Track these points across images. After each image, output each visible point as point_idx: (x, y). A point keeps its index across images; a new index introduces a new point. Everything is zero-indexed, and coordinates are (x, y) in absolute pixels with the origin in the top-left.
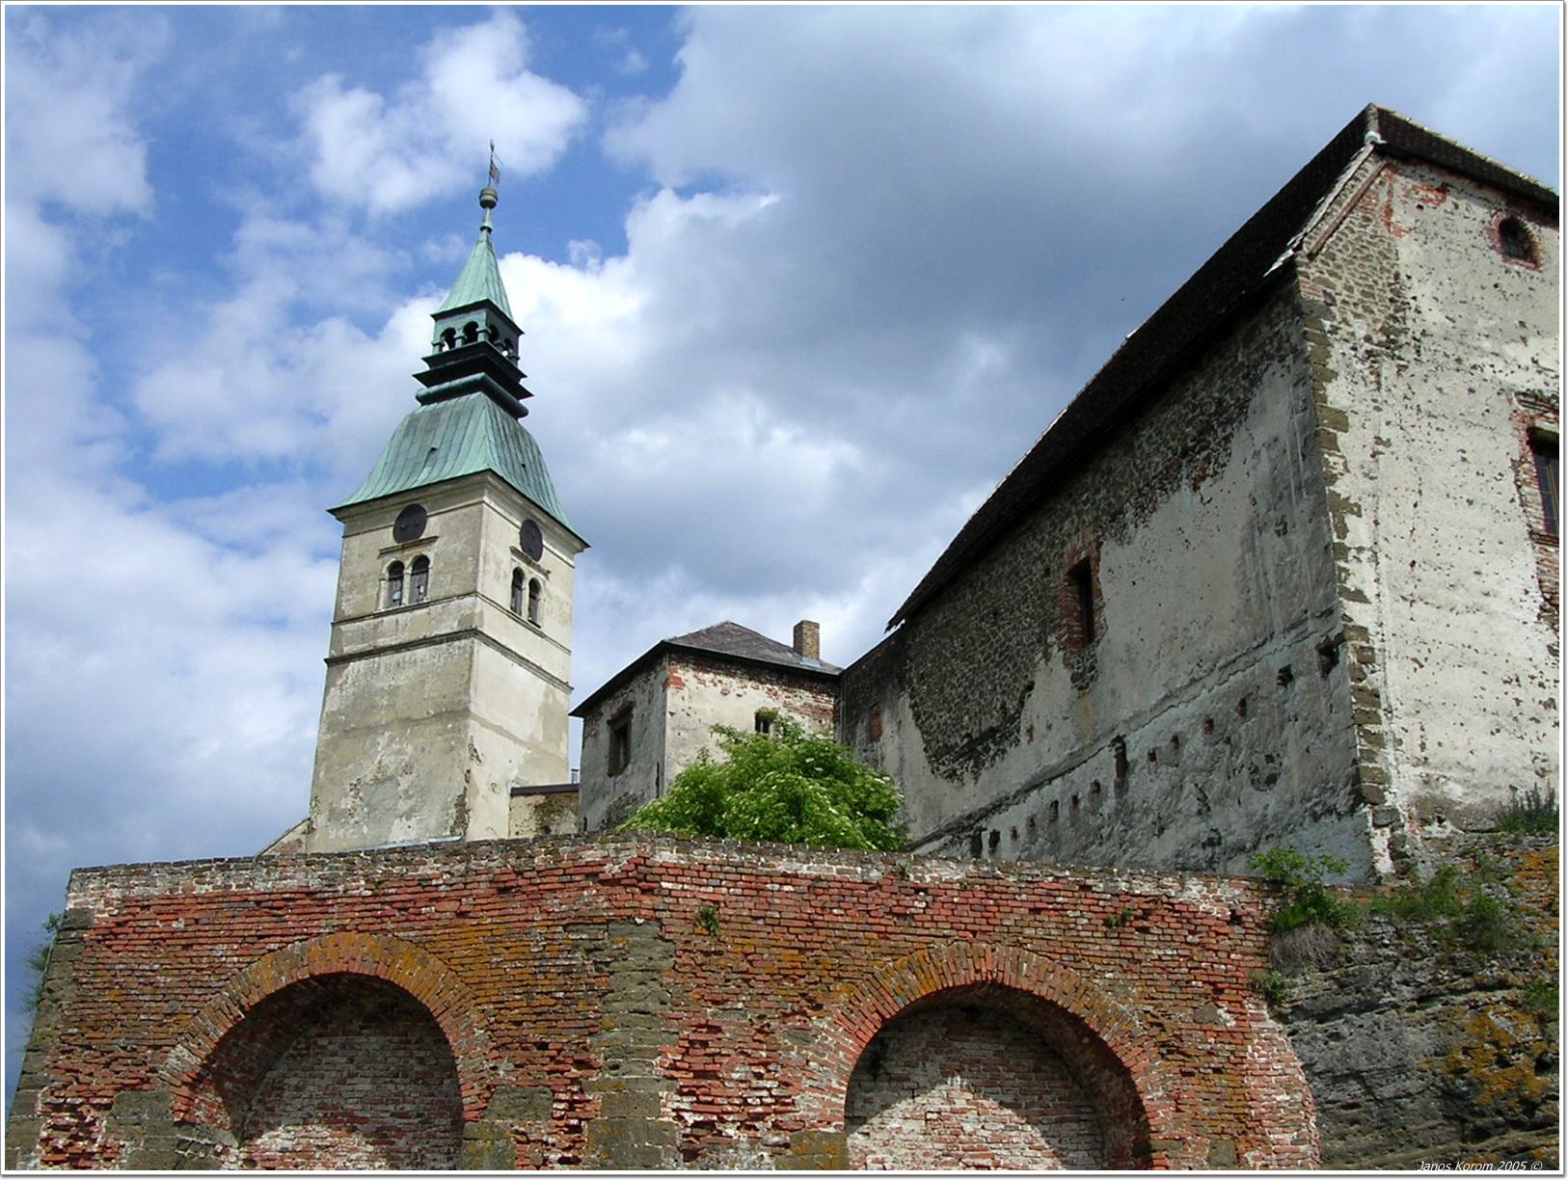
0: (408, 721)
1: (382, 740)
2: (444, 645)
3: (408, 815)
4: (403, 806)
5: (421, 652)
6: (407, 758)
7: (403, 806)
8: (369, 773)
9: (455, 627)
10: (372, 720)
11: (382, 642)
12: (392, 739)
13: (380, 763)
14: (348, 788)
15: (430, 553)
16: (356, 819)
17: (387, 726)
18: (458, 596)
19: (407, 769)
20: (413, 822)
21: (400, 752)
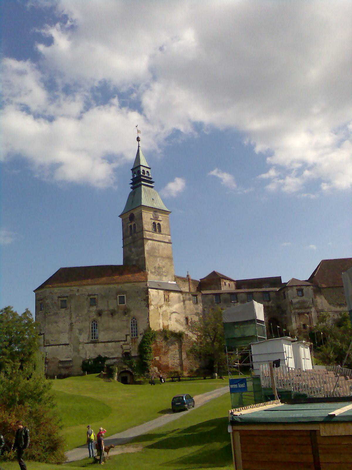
0: (162, 257)
1: (158, 259)
2: (166, 244)
3: (166, 276)
4: (165, 274)
5: (162, 244)
6: (163, 265)
7: (165, 274)
8: (157, 265)
9: (168, 241)
10: (156, 254)
11: (154, 238)
12: (160, 260)
13: (159, 264)
14: (153, 267)
15: (161, 223)
16: (156, 274)
17: (159, 257)
18: (168, 235)
19: (164, 267)
20: (167, 277)
21: (162, 263)
